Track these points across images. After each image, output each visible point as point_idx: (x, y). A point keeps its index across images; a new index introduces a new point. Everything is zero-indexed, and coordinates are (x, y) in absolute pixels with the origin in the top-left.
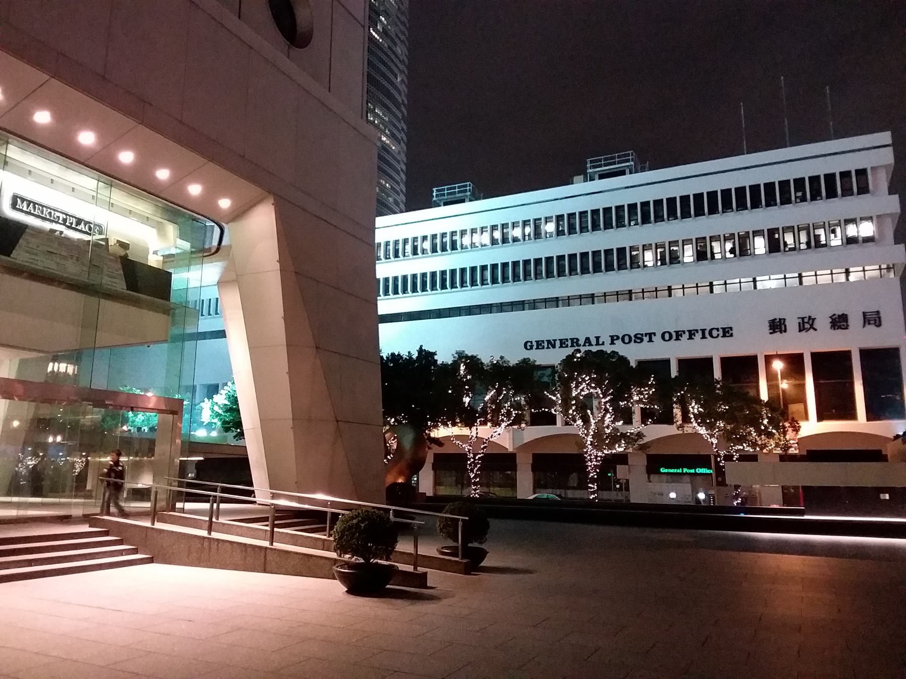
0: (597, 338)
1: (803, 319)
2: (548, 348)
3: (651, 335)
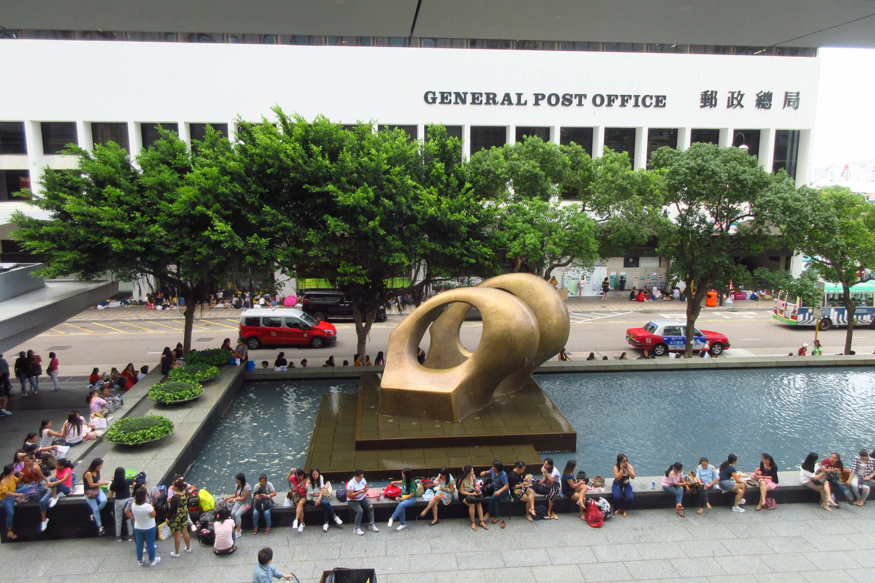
0: (519, 96)
1: (733, 93)
2: (456, 103)
3: (581, 97)
